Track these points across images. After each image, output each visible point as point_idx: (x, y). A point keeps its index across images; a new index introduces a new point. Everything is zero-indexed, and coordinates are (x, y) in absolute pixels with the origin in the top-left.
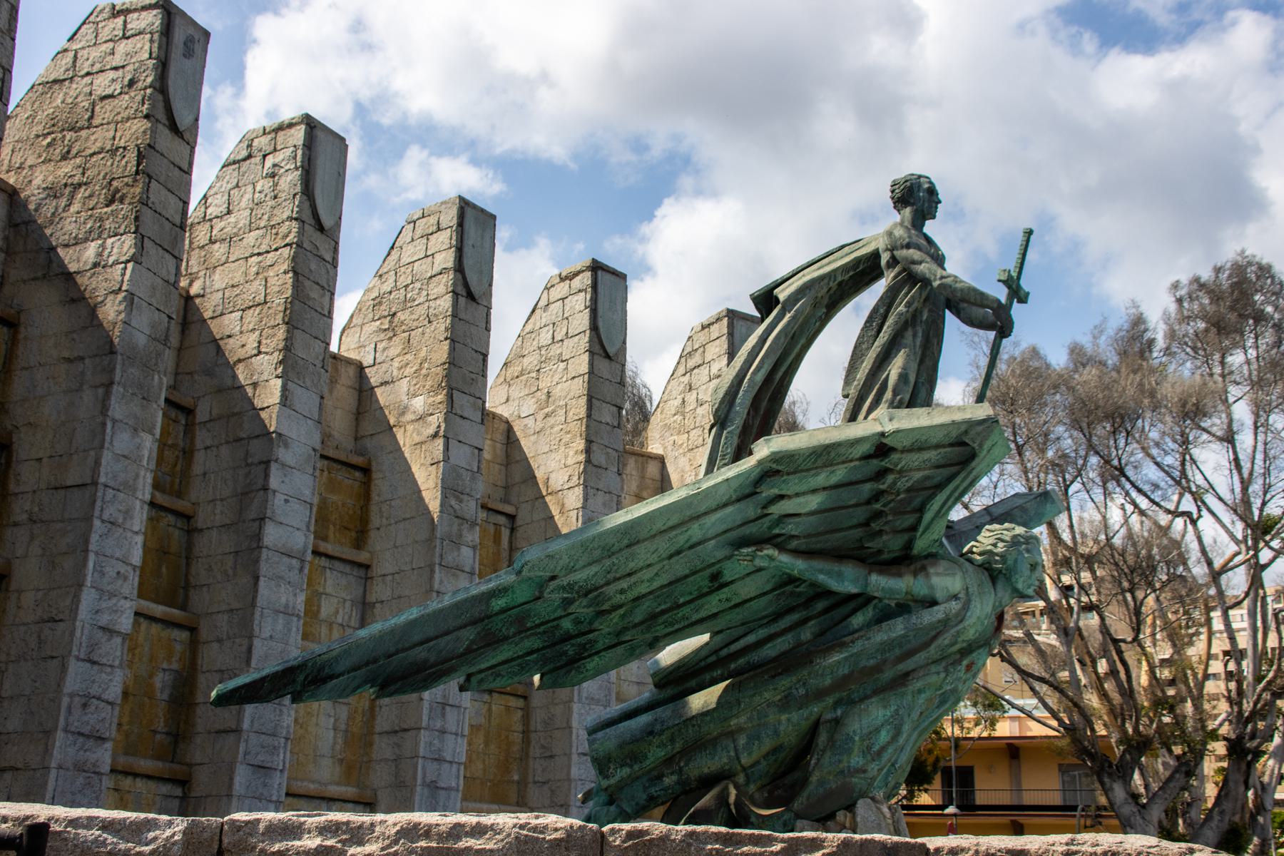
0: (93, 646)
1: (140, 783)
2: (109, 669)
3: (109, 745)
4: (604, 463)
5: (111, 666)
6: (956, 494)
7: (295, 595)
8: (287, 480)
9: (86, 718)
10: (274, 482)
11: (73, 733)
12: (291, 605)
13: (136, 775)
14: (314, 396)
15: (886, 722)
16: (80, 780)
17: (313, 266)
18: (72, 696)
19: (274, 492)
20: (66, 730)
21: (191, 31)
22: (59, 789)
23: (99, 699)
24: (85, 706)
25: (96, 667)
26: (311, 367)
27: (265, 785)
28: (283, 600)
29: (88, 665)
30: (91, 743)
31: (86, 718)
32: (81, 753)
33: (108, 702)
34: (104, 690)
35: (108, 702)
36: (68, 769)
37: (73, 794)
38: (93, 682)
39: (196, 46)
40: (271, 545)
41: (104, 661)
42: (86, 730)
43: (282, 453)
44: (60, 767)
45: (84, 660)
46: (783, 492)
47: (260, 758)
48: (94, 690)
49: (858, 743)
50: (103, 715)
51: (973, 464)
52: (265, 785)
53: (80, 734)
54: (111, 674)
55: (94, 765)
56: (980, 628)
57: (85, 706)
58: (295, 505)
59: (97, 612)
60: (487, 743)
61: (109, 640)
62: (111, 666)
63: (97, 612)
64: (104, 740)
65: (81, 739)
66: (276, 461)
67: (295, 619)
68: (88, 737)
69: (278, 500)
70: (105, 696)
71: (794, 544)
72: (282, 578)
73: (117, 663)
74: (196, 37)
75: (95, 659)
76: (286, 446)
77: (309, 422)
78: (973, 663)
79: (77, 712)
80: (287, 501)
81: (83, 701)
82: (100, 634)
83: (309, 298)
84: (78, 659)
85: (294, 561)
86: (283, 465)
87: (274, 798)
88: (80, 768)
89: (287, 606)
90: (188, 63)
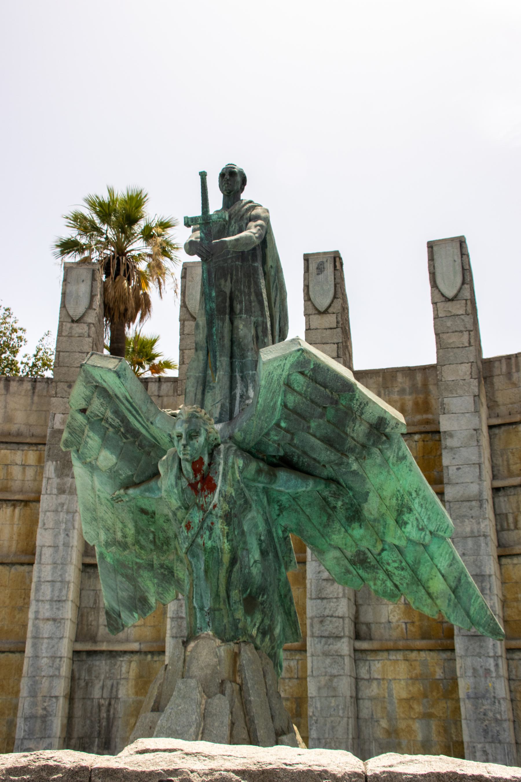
0: (320, 590)
1: (423, 654)
2: (335, 600)
3: (345, 640)
5: (336, 598)
6: (134, 412)
7: (479, 523)
8: (456, 456)
9: (323, 628)
10: (446, 461)
11: (317, 637)
12: (476, 531)
13: (419, 650)
14: (467, 398)
16: (328, 661)
17: (449, 324)
18: (312, 618)
19: (447, 467)
20: (312, 636)
22: (315, 667)
23: (332, 616)
24: (321, 622)
25: (325, 601)
26: (461, 383)
27: (481, 647)
28: (468, 529)
29: (319, 601)
30: (331, 641)
31: (324, 628)
32: (327, 646)
34: (334, 612)
35: (339, 617)
36: (318, 656)
37: (325, 668)
38: (325, 608)
39: (325, 265)
40: (451, 499)
41: (331, 596)
42: (326, 634)
43: (449, 442)
44: (312, 655)
45: (315, 599)
47: (473, 630)
48: (327, 612)
50: (337, 624)
51: (111, 393)
52: (481, 647)
53: (322, 637)
54: (336, 602)
55: (336, 651)
56: (176, 497)
57: (321, 622)
58: (466, 469)
59: (319, 572)
61: (332, 585)
62: (336, 598)
63: (319, 572)
64: (341, 637)
65: (324, 640)
66: (446, 448)
67: (482, 538)
68: (328, 637)
69: (452, 471)
70: (336, 614)
72: (465, 516)
73: (341, 595)
74: (325, 260)
75: (323, 596)
76: (451, 436)
77: (467, 415)
78: (189, 523)
79: (317, 626)
80: (458, 469)
81: (321, 619)
82: (325, 583)
83: (450, 344)
84: (311, 599)
85: (474, 503)
86: (452, 449)
87: (491, 654)
88: (326, 654)
89: (472, 532)
90: (321, 276)
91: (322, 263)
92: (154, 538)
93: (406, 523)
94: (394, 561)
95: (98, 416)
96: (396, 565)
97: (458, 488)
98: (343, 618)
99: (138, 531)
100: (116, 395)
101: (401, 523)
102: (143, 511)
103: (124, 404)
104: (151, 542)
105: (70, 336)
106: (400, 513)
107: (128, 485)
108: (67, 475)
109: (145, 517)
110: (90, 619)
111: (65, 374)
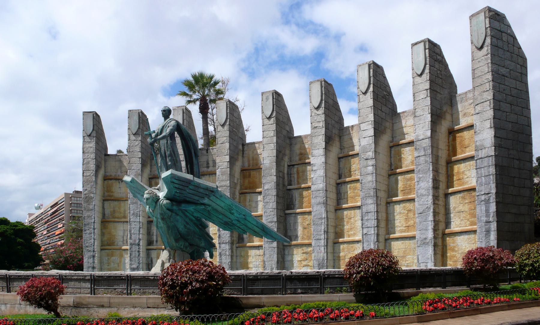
76: (315, 166)
97: (316, 186)
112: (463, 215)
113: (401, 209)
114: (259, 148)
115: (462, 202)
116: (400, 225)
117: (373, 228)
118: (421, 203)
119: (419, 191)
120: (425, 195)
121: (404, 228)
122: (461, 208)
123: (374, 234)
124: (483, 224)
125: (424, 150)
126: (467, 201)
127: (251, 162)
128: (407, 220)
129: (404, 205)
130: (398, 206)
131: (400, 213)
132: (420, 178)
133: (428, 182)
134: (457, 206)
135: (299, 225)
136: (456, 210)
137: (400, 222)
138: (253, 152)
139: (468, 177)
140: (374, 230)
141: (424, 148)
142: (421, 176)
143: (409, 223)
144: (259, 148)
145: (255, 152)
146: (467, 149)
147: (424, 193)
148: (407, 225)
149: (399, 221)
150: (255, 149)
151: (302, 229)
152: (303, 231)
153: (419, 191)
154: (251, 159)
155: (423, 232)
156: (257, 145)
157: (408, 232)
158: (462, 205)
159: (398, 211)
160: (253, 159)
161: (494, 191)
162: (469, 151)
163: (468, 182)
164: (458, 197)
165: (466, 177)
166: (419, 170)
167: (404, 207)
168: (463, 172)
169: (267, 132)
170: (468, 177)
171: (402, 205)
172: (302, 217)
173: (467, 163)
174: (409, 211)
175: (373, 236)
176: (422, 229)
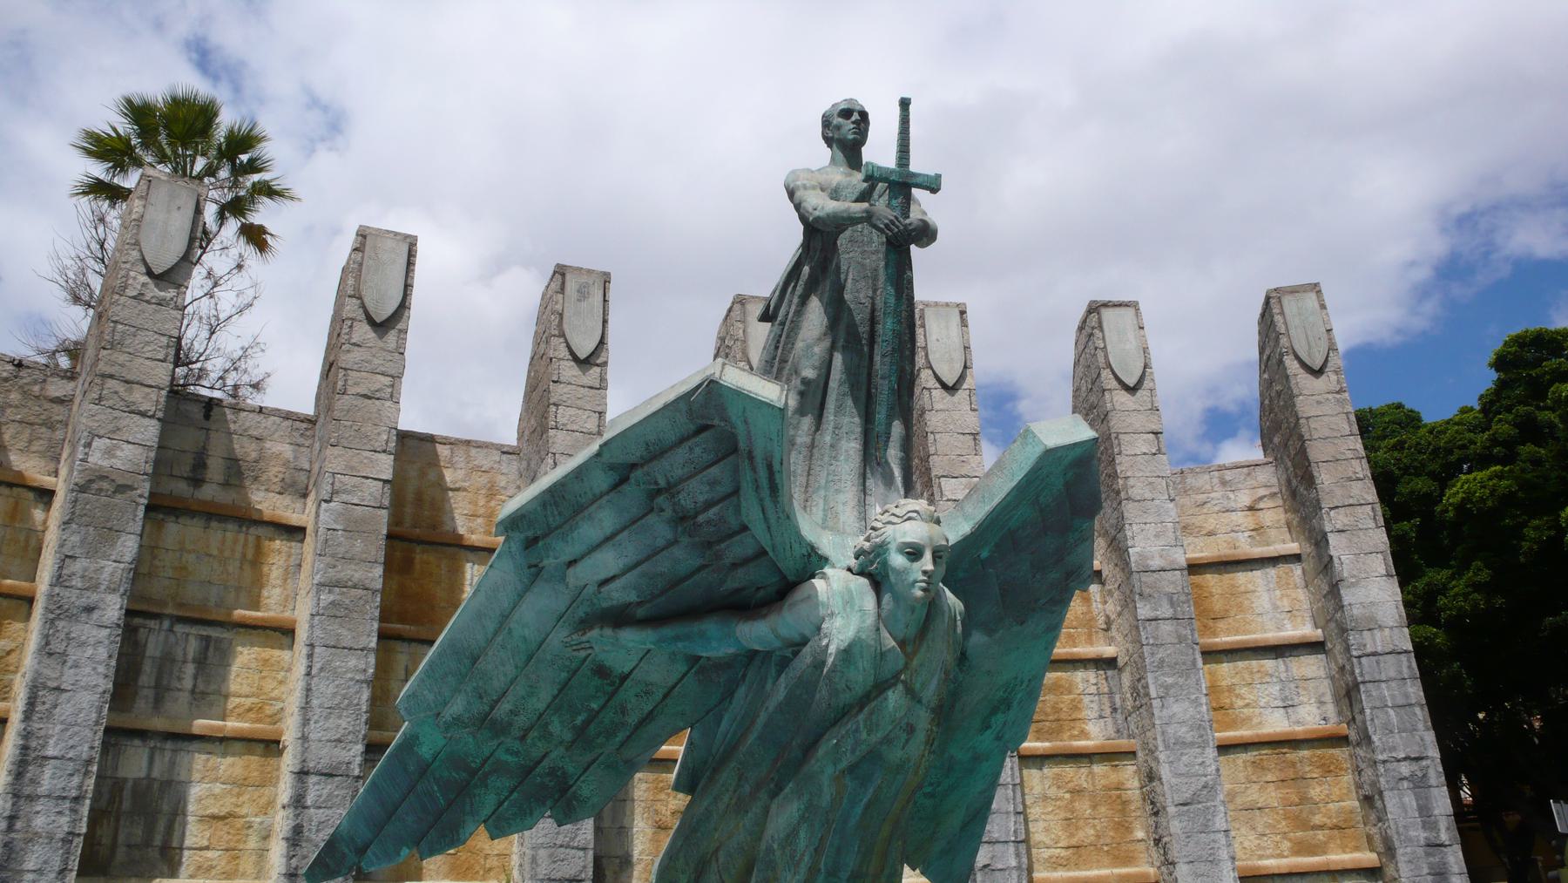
4: (1148, 495)
15: (802, 818)
21: (584, 279)
33: (578, 848)
34: (573, 839)
46: (567, 558)
49: (778, 853)
51: (742, 445)
60: (1094, 807)
71: (641, 612)
90: (584, 304)
91: (586, 285)
92: (587, 723)
93: (989, 727)
94: (931, 784)
95: (656, 483)
96: (928, 789)
98: (584, 849)
99: (555, 706)
100: (750, 452)
101: (986, 726)
102: (601, 671)
103: (754, 470)
104: (574, 727)
105: (138, 297)
106: (994, 711)
107: (619, 618)
108: (106, 557)
109: (597, 681)
110: (99, 832)
111: (122, 366)
112: (1261, 821)
113: (1047, 783)
114: (452, 465)
115: (1254, 778)
116: (1048, 842)
117: (1011, 848)
118: (1183, 770)
119: (1170, 730)
120: (1192, 744)
121: (1064, 853)
122: (1254, 795)
123: (1019, 868)
124: (1420, 851)
125: (1172, 604)
126: (1270, 777)
127: (408, 510)
128: (1070, 823)
129: (1056, 770)
130: (1034, 772)
131: (1045, 798)
132: (1167, 688)
133: (1196, 703)
134: (1238, 788)
135: (638, 810)
136: (1239, 800)
137: (1047, 830)
138: (423, 474)
139: (1247, 705)
140: (1018, 855)
141: (1170, 597)
142: (1170, 680)
143: (1081, 834)
144: (452, 465)
145: (432, 476)
146: (1221, 625)
147: (1189, 738)
148: (1074, 841)
149: (1041, 825)
150: (434, 462)
151: (649, 831)
152: (655, 840)
153: (1170, 730)
154: (410, 496)
155: (1203, 868)
156: (443, 451)
157: (1077, 866)
158: (1256, 787)
159: (1037, 789)
160: (419, 499)
161: (1434, 753)
162: (1228, 632)
163: (1249, 719)
164: (1240, 762)
165: (1240, 703)
166: (1162, 661)
167: (1058, 776)
168: (1231, 689)
169: (572, 411)
170: (1247, 705)
171: (1050, 771)
172: (651, 776)
173: (1240, 664)
174: (1077, 792)
175: (1015, 874)
176: (1199, 860)
